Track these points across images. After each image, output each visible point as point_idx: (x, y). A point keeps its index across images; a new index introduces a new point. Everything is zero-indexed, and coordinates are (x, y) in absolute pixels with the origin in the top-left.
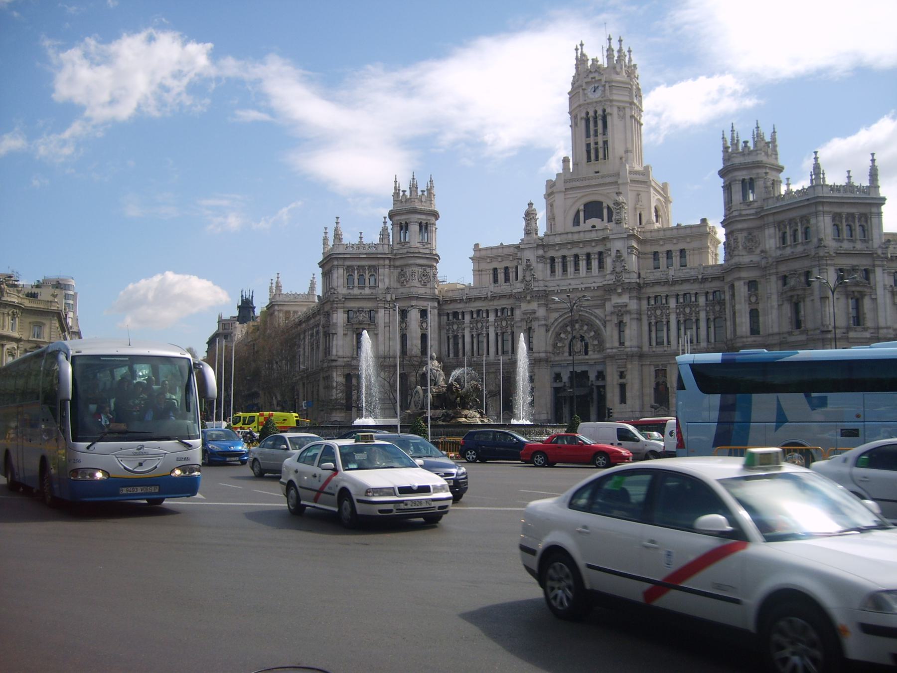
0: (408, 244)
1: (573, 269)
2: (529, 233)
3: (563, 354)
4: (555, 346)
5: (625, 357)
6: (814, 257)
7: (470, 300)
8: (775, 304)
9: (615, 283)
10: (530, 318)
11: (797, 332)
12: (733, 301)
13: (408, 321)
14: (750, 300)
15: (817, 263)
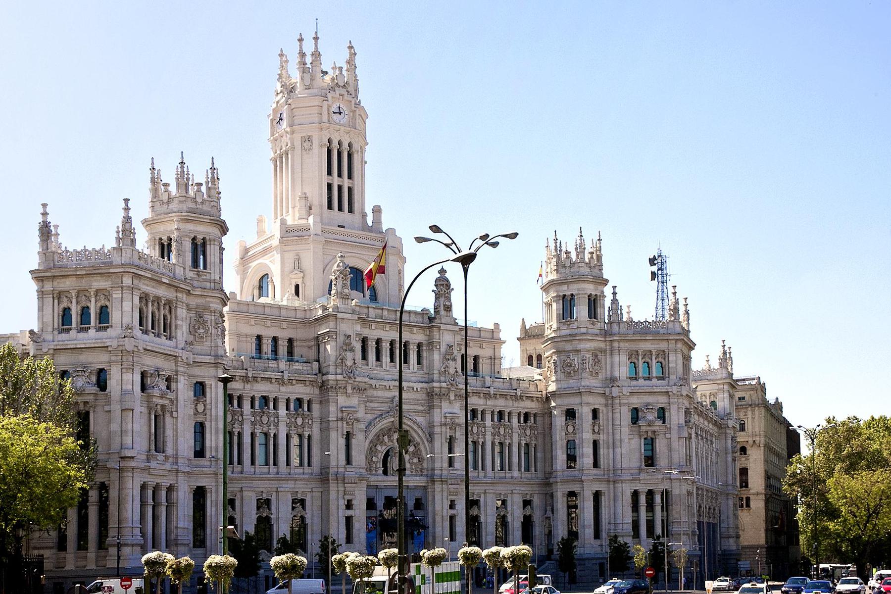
0: (207, 275)
1: (388, 359)
2: (346, 298)
3: (376, 471)
4: (370, 461)
5: (459, 482)
6: (674, 394)
7: (255, 378)
8: (625, 437)
9: (449, 387)
10: (346, 416)
11: (651, 469)
12: (571, 429)
13: (208, 401)
14: (594, 430)
15: (676, 400)
